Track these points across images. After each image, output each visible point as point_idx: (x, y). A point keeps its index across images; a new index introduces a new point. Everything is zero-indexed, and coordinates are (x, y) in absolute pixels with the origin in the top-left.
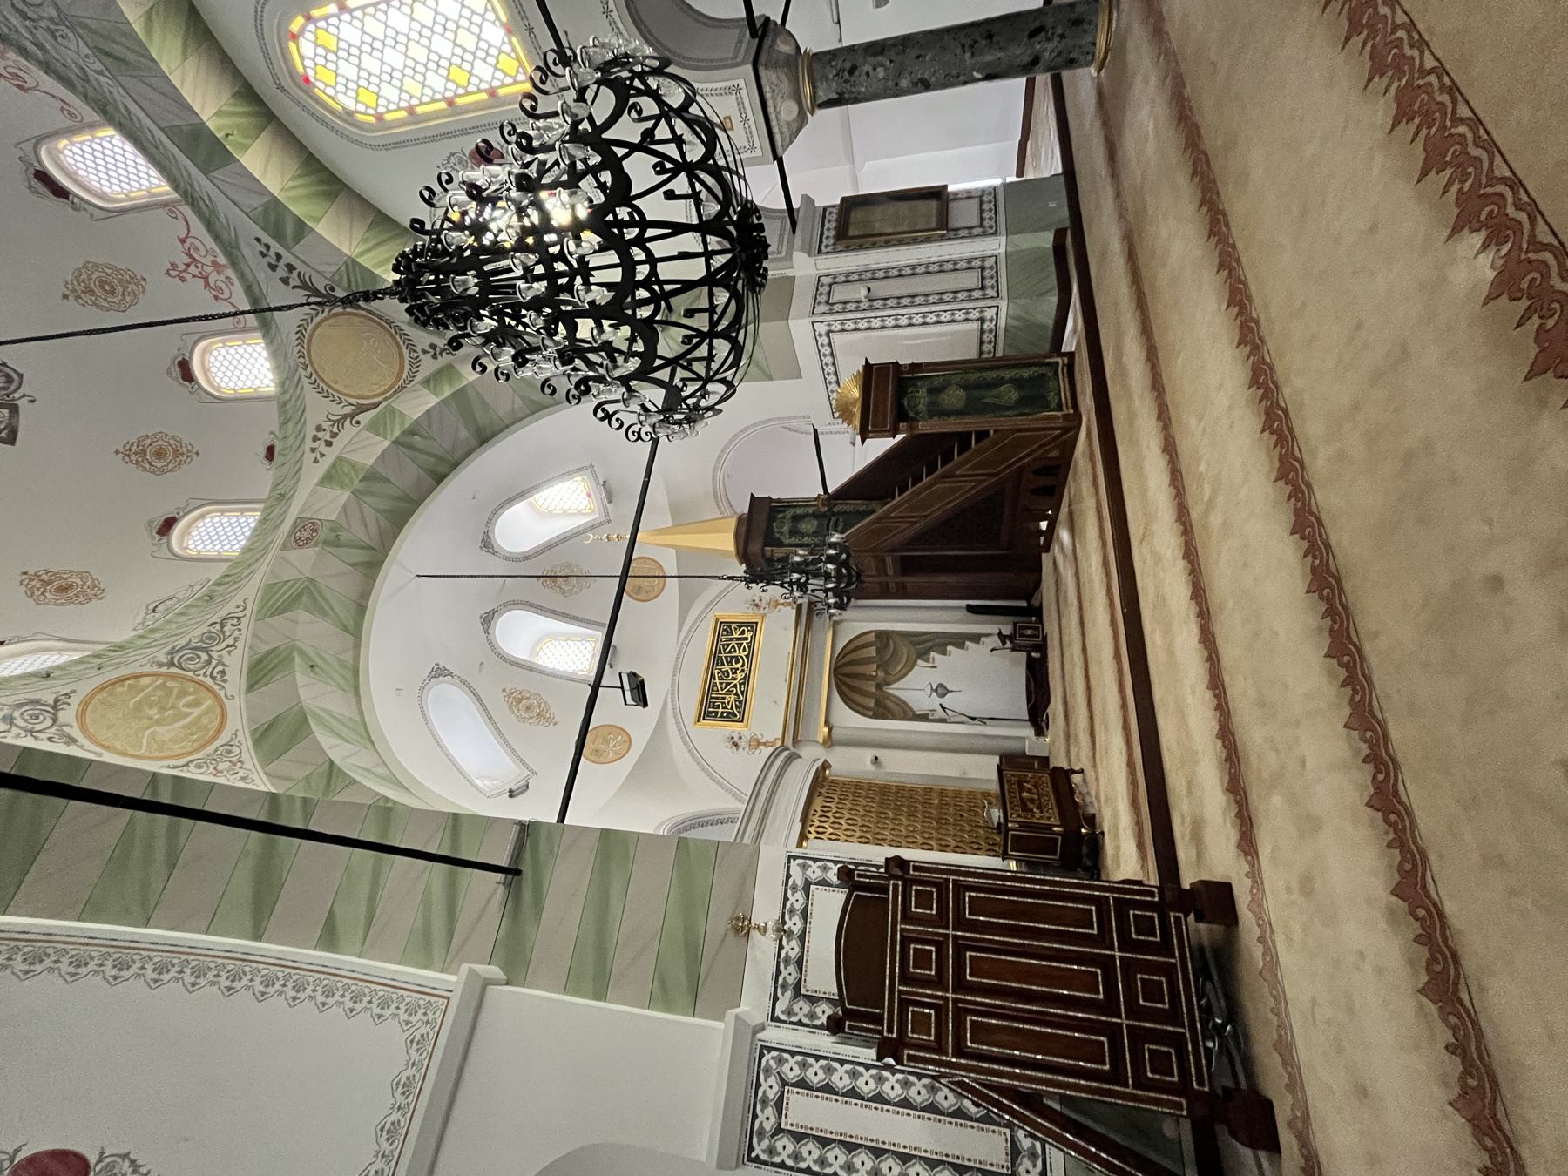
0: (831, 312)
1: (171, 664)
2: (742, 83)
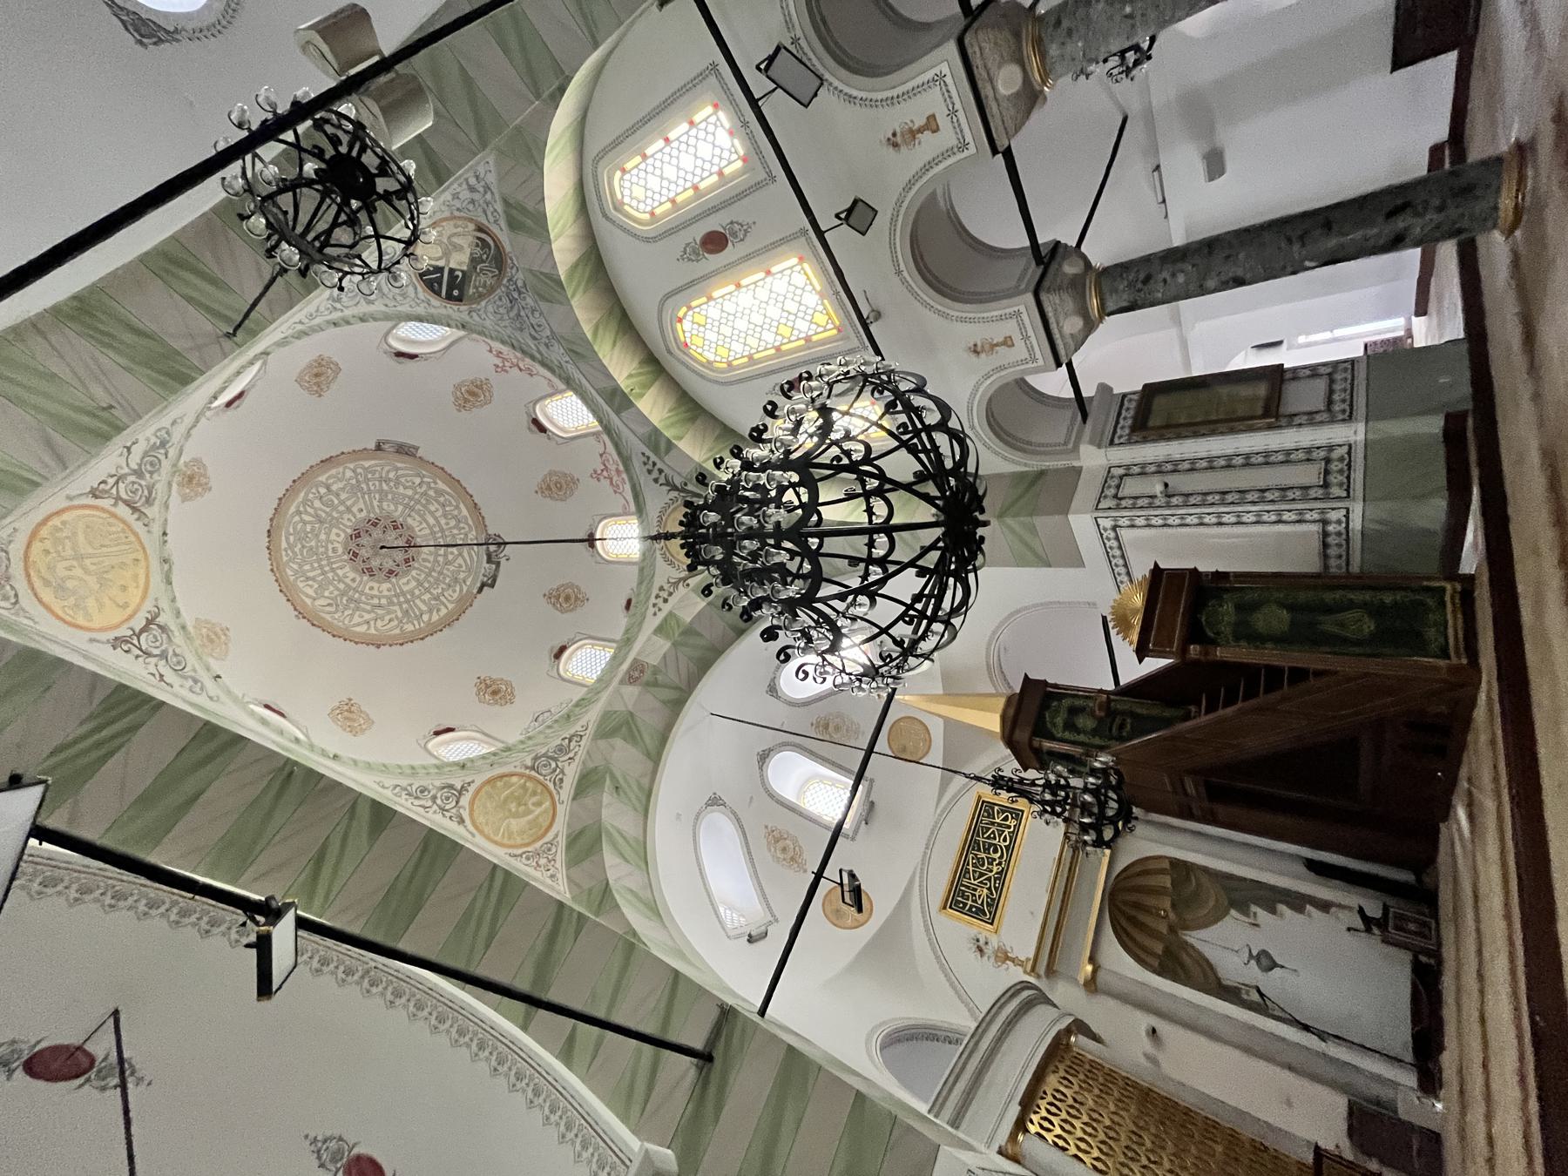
0: (1118, 508)
1: (533, 768)
2: (1022, 309)
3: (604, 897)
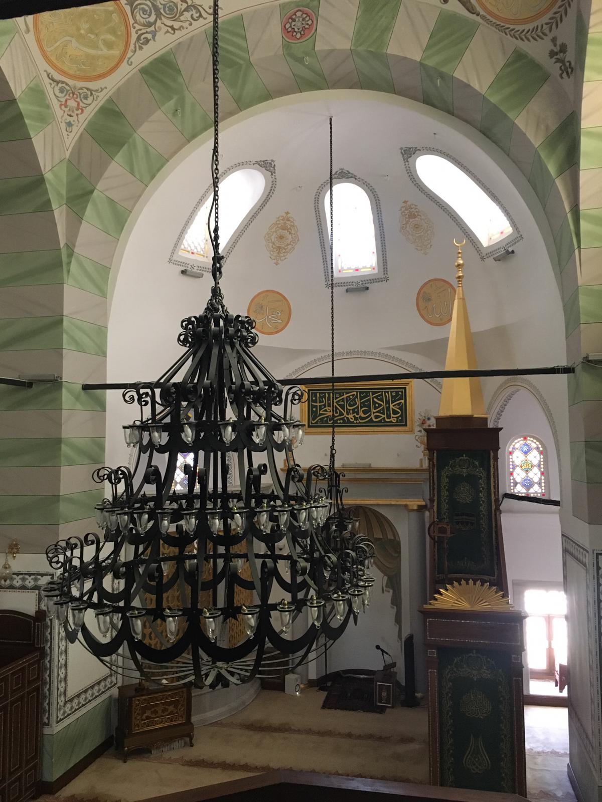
3: (79, 197)
